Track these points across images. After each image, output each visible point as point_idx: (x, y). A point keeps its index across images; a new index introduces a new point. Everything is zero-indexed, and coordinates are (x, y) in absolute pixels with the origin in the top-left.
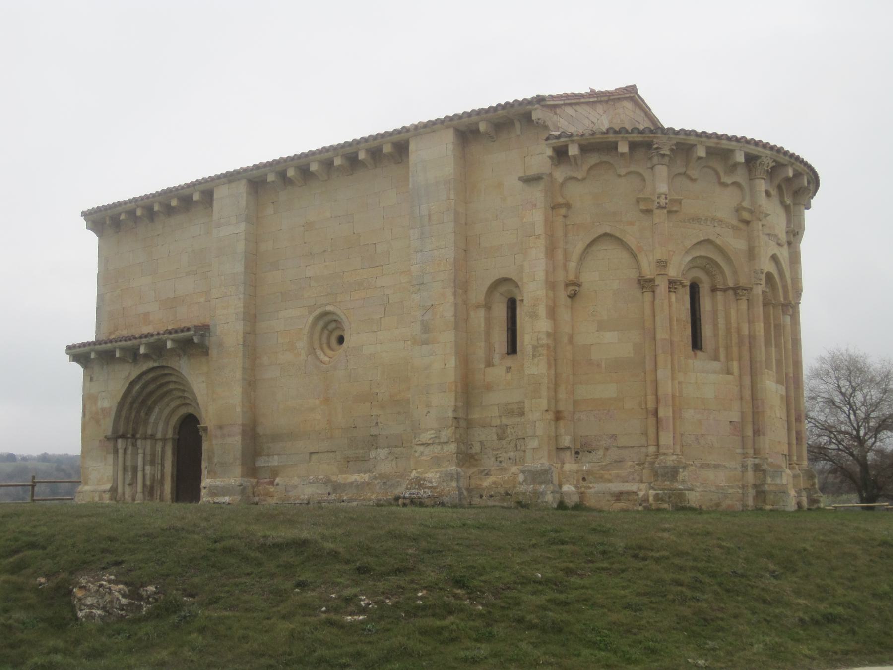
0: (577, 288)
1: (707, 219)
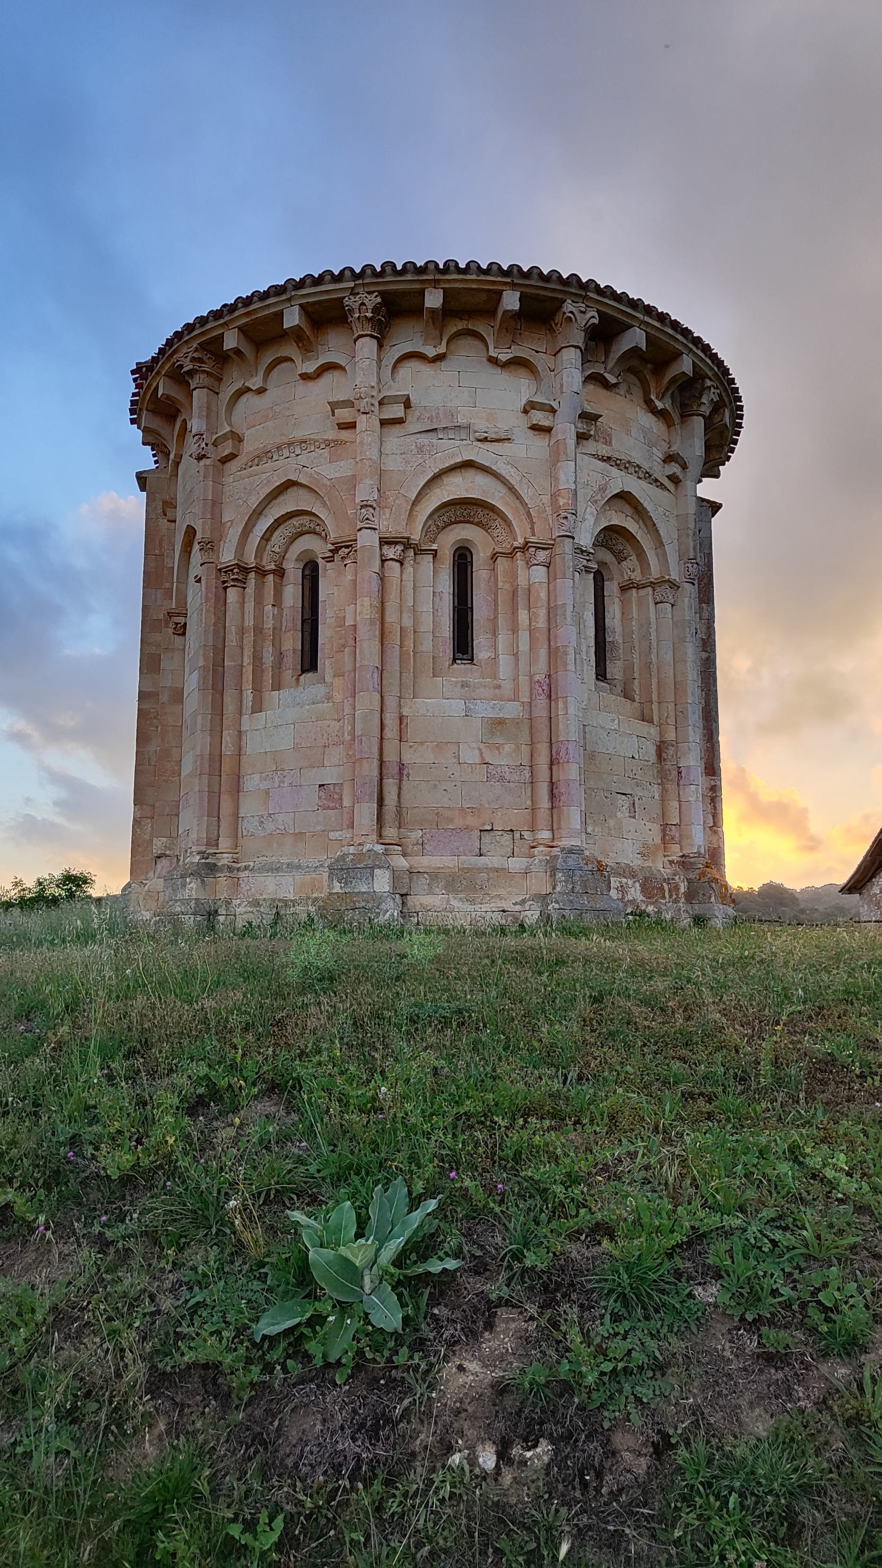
0: (181, 620)
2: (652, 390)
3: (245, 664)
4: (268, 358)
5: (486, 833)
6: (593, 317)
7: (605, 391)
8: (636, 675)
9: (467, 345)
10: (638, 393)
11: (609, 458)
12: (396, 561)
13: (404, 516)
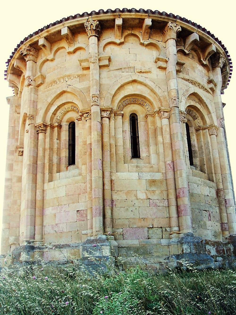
1: (59, 79)
2: (201, 57)
3: (45, 163)
4: (55, 48)
5: (150, 229)
6: (179, 28)
7: (185, 56)
8: (205, 163)
9: (132, 39)
10: (196, 58)
11: (188, 80)
12: (107, 117)
13: (110, 100)
